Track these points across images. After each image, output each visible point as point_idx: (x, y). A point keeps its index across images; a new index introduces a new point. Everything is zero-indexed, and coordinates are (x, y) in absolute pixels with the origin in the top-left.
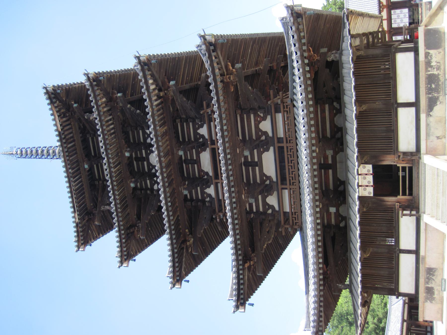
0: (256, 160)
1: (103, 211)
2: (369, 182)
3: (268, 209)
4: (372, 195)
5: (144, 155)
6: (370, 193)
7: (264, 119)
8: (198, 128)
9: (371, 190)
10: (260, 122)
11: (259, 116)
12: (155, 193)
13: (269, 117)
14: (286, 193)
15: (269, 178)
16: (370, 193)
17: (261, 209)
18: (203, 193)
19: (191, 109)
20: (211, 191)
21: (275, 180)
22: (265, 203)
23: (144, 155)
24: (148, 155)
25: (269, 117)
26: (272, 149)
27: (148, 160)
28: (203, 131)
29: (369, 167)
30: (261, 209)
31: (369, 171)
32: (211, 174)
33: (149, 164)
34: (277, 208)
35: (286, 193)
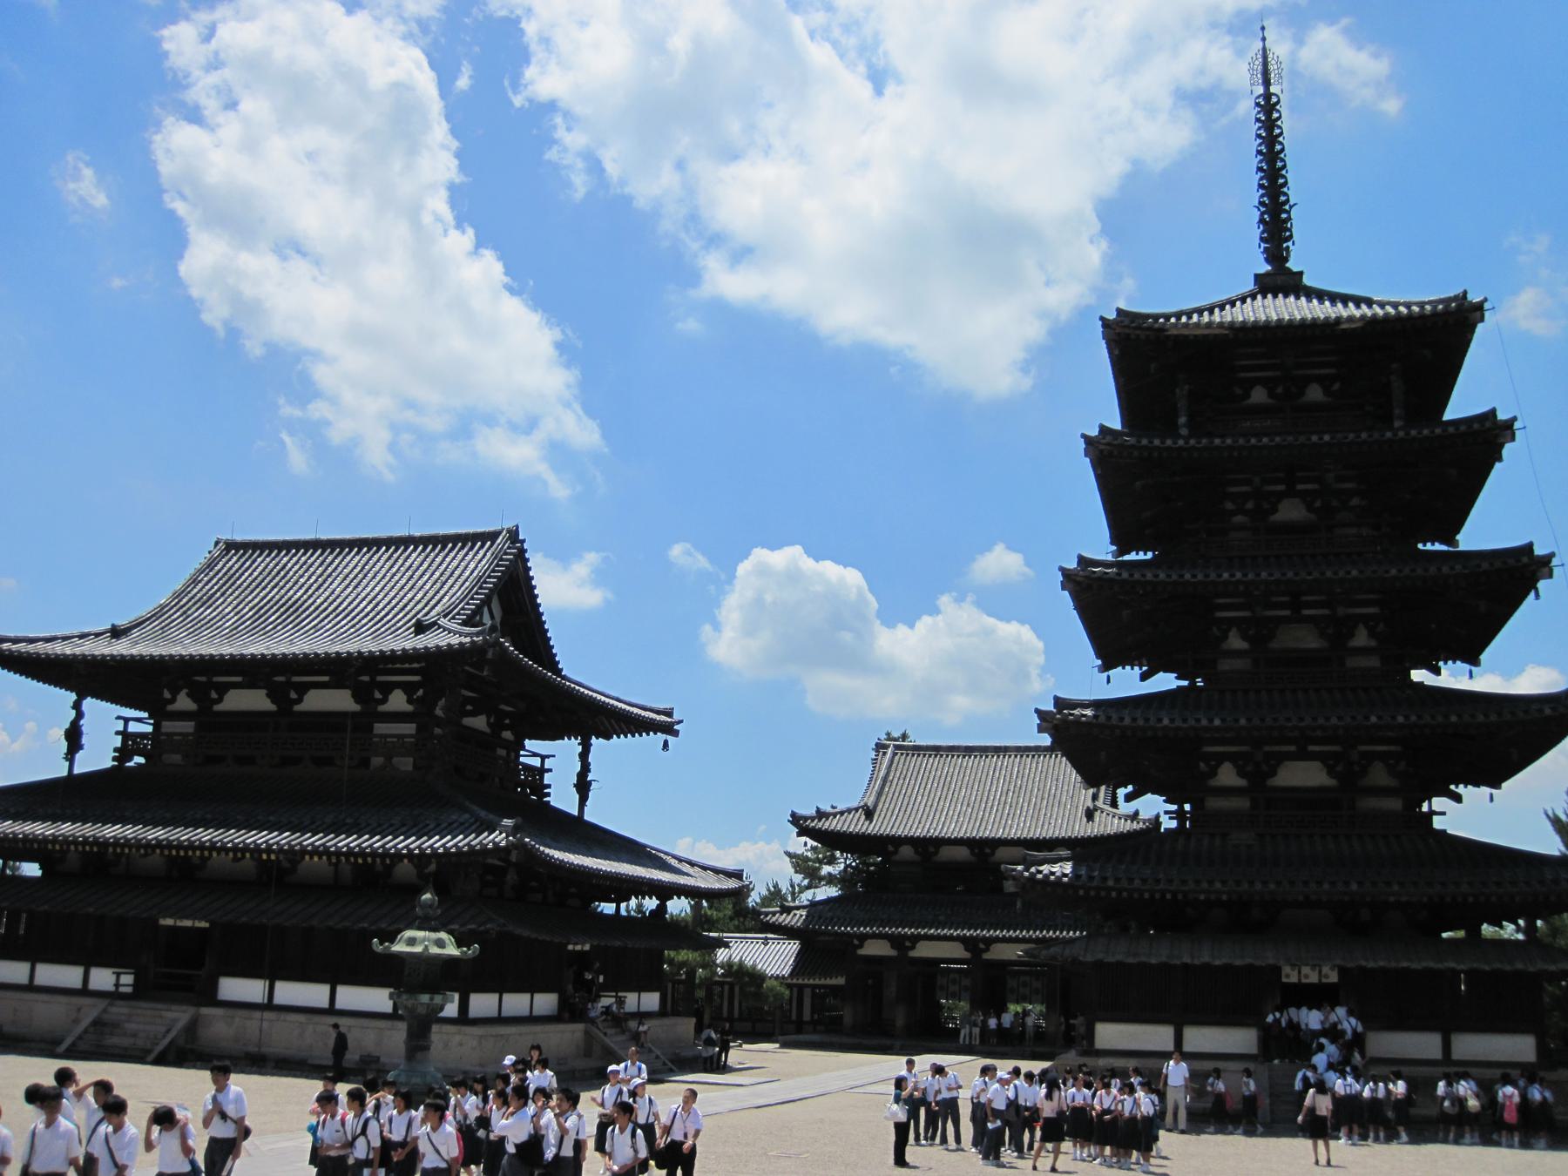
0: (1312, 748)
2: (1307, 976)
4: (1284, 980)
5: (1300, 487)
6: (1288, 976)
9: (1294, 979)
14: (1243, 803)
15: (1273, 773)
16: (1288, 976)
22: (1221, 758)
23: (1300, 487)
27: (1291, 493)
29: (1333, 977)
31: (1327, 976)
33: (1281, 496)
35: (1243, 803)
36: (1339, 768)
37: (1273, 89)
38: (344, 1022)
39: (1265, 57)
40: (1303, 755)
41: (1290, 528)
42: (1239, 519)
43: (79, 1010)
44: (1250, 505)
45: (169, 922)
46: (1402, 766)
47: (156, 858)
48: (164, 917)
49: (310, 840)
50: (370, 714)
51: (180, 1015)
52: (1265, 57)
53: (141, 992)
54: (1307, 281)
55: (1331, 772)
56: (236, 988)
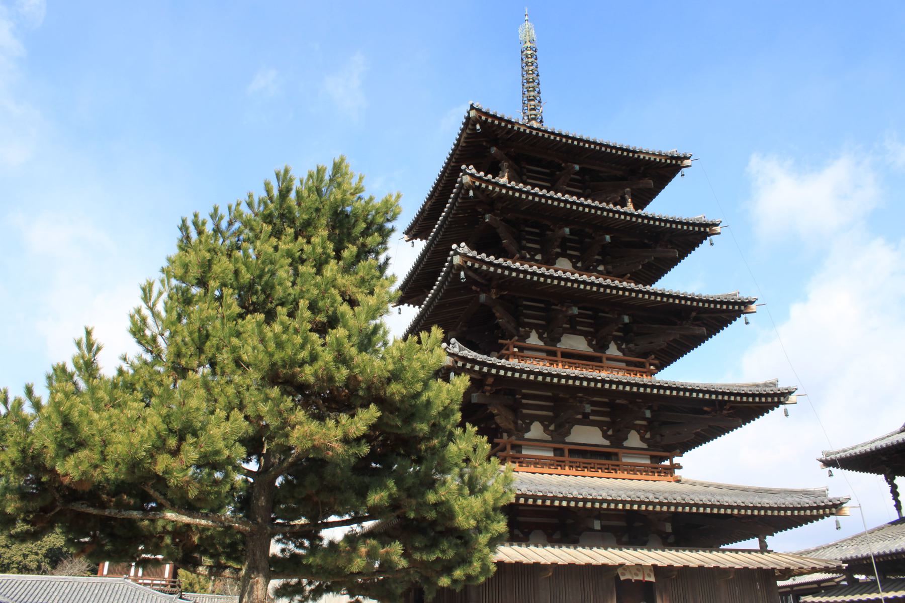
1: (499, 162)
3: (524, 422)
5: (569, 252)
7: (643, 439)
8: (616, 344)
10: (639, 433)
11: (646, 432)
12: (523, 252)
13: (645, 446)
15: (568, 433)
17: (525, 411)
18: (532, 326)
19: (651, 343)
20: (534, 340)
21: (568, 439)
23: (569, 252)
24: (570, 258)
25: (645, 446)
26: (607, 442)
27: (563, 255)
28: (613, 350)
30: (525, 411)
32: (559, 345)
34: (527, 435)
36: (610, 433)
40: (586, 421)
44: (538, 257)
46: (648, 436)
55: (605, 436)
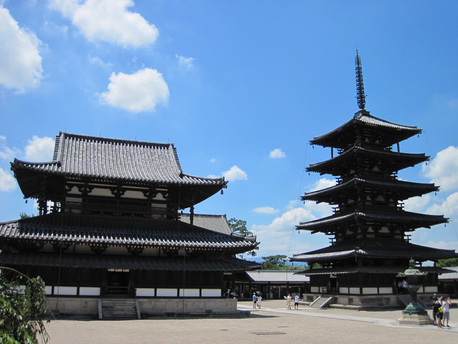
37: (360, 66)
38: (351, 297)
39: (358, 58)
41: (376, 173)
42: (366, 169)
43: (86, 303)
45: (112, 270)
47: (88, 248)
48: (110, 268)
49: (181, 243)
50: (150, 201)
51: (130, 302)
52: (358, 58)
53: (103, 295)
54: (370, 114)
56: (140, 292)
